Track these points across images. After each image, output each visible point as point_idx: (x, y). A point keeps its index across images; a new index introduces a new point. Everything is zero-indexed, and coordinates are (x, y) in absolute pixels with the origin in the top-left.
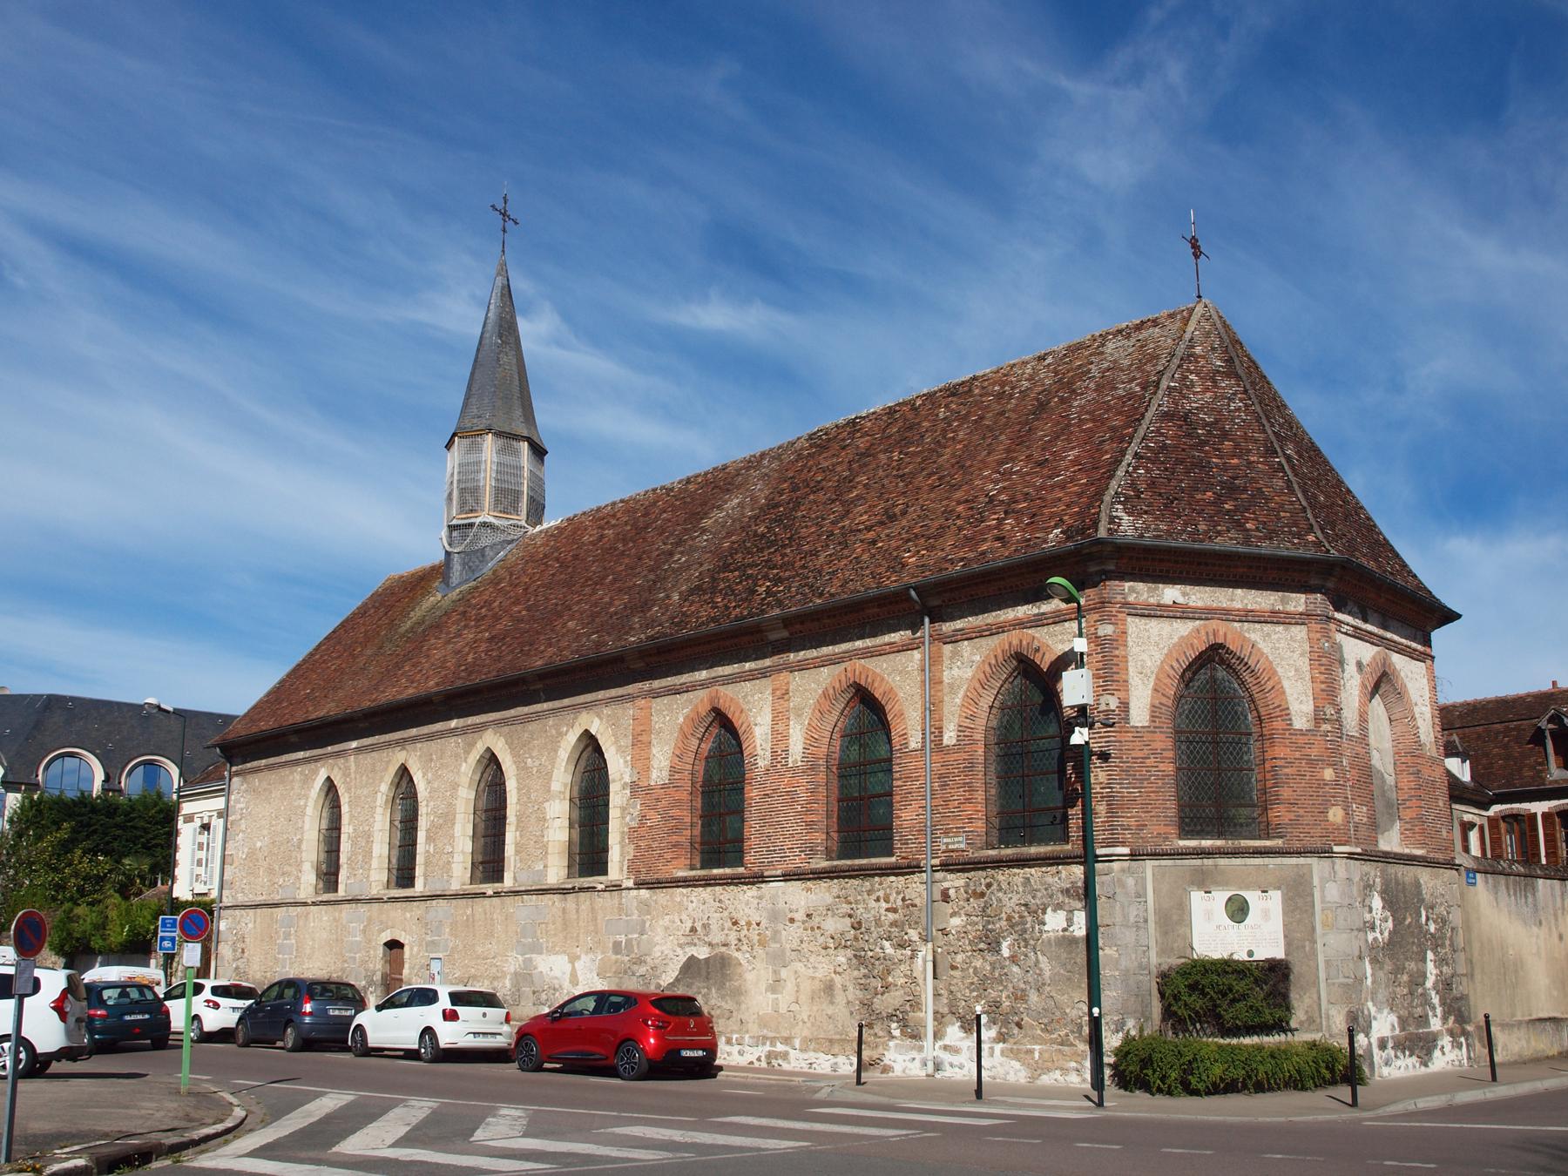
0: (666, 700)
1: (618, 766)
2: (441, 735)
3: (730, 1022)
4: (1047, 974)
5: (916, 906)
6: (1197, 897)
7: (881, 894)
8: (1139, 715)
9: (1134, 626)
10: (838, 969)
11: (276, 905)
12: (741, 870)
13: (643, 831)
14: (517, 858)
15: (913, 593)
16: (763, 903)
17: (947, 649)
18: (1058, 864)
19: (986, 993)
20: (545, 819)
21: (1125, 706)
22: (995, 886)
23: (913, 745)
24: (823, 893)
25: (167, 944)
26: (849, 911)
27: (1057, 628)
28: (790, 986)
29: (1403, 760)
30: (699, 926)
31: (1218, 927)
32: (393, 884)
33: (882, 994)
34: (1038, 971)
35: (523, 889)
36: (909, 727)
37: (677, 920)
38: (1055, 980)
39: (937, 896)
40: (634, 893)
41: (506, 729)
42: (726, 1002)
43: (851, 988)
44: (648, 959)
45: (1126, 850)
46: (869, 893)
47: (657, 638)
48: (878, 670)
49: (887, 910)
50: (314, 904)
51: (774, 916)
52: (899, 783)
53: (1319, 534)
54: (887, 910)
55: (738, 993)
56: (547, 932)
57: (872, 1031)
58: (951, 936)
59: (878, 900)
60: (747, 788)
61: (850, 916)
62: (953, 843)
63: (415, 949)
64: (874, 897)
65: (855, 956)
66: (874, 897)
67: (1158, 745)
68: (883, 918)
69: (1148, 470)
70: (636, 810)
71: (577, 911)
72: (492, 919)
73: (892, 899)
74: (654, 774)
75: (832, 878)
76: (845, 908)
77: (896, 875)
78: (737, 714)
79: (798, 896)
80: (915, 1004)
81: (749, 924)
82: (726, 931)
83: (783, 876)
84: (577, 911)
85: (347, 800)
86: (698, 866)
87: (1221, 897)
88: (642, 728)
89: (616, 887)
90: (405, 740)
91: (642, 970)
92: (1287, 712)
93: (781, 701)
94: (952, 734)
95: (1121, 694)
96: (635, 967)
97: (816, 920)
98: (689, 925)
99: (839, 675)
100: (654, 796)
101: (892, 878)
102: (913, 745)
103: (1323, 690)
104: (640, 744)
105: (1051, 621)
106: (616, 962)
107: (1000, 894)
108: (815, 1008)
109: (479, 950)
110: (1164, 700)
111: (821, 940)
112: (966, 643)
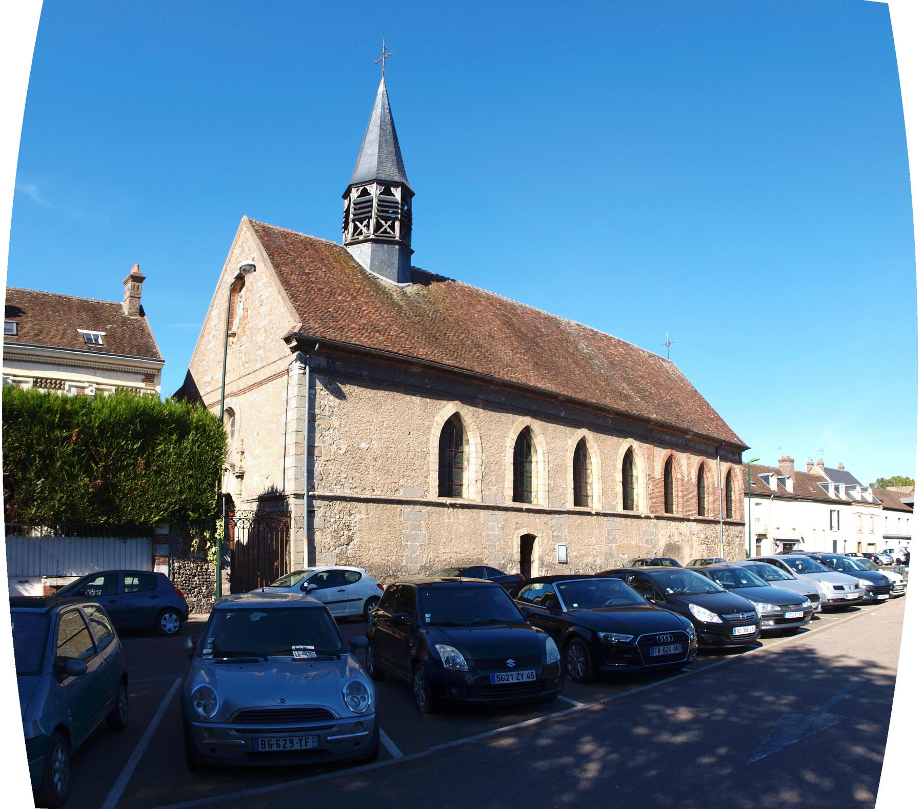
44: (657, 546)
56: (619, 533)
98: (668, 534)
100: (657, 482)
106: (647, 548)
109: (586, 541)
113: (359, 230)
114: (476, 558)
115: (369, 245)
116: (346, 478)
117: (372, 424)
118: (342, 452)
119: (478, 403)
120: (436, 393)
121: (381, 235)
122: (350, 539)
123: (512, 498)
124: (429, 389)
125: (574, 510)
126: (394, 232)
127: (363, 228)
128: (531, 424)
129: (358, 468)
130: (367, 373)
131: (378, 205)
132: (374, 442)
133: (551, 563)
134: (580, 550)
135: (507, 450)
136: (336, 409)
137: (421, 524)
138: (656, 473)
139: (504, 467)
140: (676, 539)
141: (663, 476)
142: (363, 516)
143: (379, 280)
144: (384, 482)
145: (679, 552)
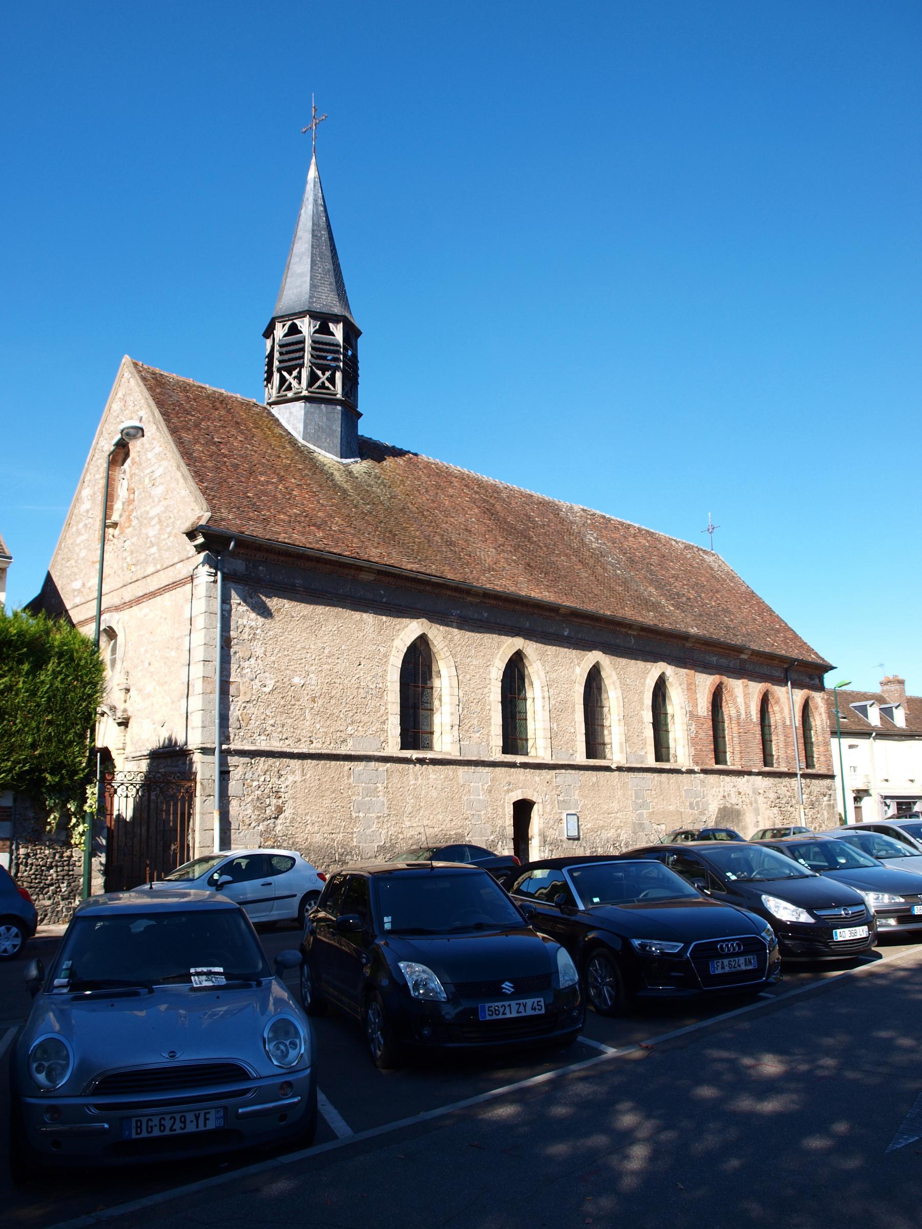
14: (627, 744)
44: (706, 812)
56: (651, 795)
96: (701, 817)
98: (722, 794)
100: (701, 722)
113: (287, 383)
114: (455, 834)
115: (300, 405)
116: (274, 726)
117: (309, 651)
118: (267, 690)
119: (451, 621)
120: (395, 608)
121: (317, 391)
122: (280, 810)
123: (501, 748)
124: (385, 603)
125: (586, 764)
126: (334, 387)
127: (292, 381)
128: (523, 648)
129: (290, 711)
130: (302, 582)
131: (313, 348)
132: (312, 675)
133: (557, 839)
134: (597, 819)
135: (492, 684)
136: (258, 631)
137: (377, 787)
138: (699, 710)
139: (488, 707)
140: (734, 801)
141: (710, 713)
142: (298, 778)
143: (315, 454)
144: (325, 730)
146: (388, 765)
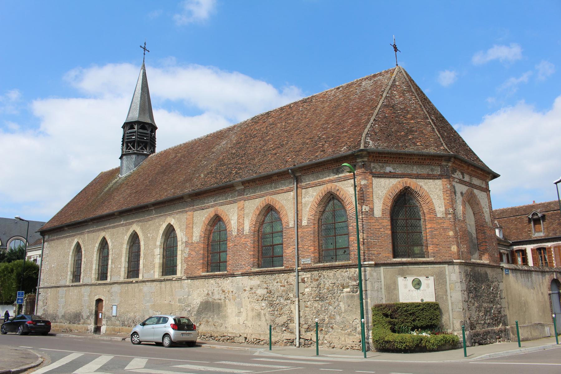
0: (198, 212)
1: (180, 235)
2: (118, 226)
3: (222, 328)
4: (343, 309)
5: (292, 284)
6: (400, 280)
7: (278, 280)
8: (378, 213)
9: (376, 181)
10: (262, 308)
11: (58, 287)
12: (226, 272)
13: (189, 259)
14: (144, 269)
15: (290, 171)
16: (234, 284)
17: (304, 190)
18: (347, 268)
19: (319, 316)
20: (154, 255)
21: (372, 210)
22: (322, 276)
23: (291, 226)
24: (256, 281)
25: (20, 301)
26: (267, 287)
27: (345, 182)
28: (244, 314)
29: (479, 228)
30: (210, 292)
31: (409, 290)
32: (99, 279)
33: (279, 317)
34: (339, 308)
35: (146, 280)
36: (289, 219)
37: (202, 291)
38: (346, 311)
39: (300, 281)
40: (187, 281)
41: (141, 224)
42: (220, 320)
43: (267, 315)
45: (373, 263)
46: (274, 280)
47: (196, 190)
48: (277, 199)
49: (281, 286)
50: (72, 286)
51: (238, 289)
52: (285, 240)
53: (445, 146)
54: (281, 286)
55: (225, 317)
56: (154, 295)
57: (275, 331)
58: (305, 296)
59: (277, 282)
60: (228, 243)
61: (267, 289)
62: (306, 261)
63: (107, 302)
64: (276, 281)
65: (269, 303)
66: (276, 281)
67: (385, 224)
68: (279, 289)
69: (379, 125)
70: (187, 250)
71: (165, 288)
72: (135, 291)
73: (283, 282)
74: (194, 238)
75: (260, 275)
76: (265, 286)
77: (284, 273)
78: (224, 216)
79: (247, 282)
80: (291, 320)
81: (229, 292)
82: (220, 295)
83: (242, 274)
84: (165, 288)
85: (84, 250)
86: (210, 271)
87: (410, 279)
88: (189, 222)
89: (180, 279)
90: (105, 228)
91: (189, 309)
92: (435, 211)
93: (241, 211)
94: (305, 221)
95: (371, 205)
96: (186, 308)
97: (253, 291)
98: (206, 292)
99: (263, 201)
101: (283, 274)
102: (291, 226)
103: (448, 203)
104: (189, 227)
105: (343, 180)
106: (179, 306)
107: (324, 280)
108: (254, 322)
109: (130, 302)
110: (387, 207)
111: (256, 297)
112: (311, 188)
140: (216, 297)
145: (219, 310)
146: (66, 288)
